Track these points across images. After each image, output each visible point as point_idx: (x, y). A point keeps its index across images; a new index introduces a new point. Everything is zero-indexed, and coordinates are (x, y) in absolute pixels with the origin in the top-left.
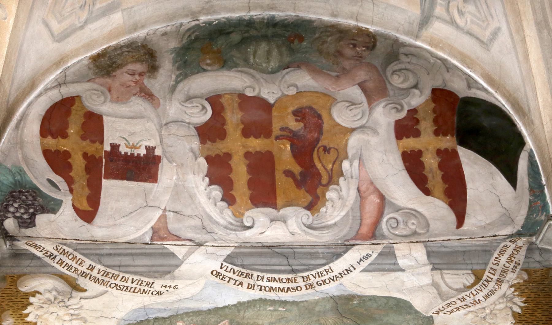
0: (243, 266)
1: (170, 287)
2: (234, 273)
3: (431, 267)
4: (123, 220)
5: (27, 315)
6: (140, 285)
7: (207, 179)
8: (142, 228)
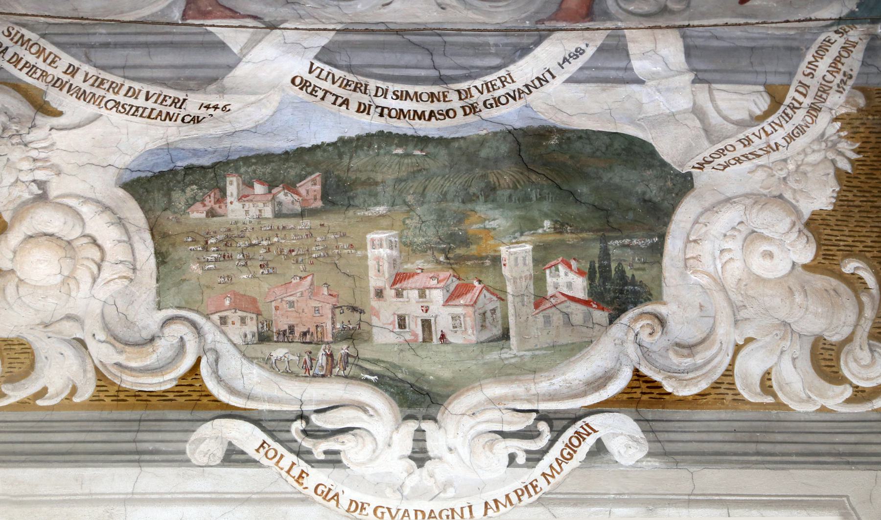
0: (350, 69)
2: (334, 83)
3: (690, 77)
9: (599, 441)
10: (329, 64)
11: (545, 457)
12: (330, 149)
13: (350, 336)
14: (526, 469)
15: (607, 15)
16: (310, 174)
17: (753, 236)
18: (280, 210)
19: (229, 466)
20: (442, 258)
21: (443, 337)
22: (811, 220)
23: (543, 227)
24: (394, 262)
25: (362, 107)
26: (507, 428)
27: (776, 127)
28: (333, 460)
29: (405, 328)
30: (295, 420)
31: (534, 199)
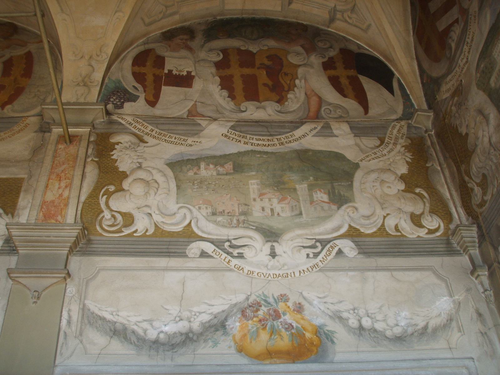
0: (241, 132)
1: (197, 142)
3: (353, 135)
5: (113, 155)
7: (220, 87)
9: (340, 249)
10: (234, 130)
11: (320, 255)
13: (244, 213)
14: (313, 259)
15: (324, 118)
16: (229, 162)
17: (383, 182)
19: (202, 258)
20: (276, 189)
21: (278, 214)
22: (401, 176)
23: (310, 179)
24: (259, 190)
25: (245, 143)
26: (305, 245)
28: (241, 256)
29: (264, 211)
30: (226, 242)
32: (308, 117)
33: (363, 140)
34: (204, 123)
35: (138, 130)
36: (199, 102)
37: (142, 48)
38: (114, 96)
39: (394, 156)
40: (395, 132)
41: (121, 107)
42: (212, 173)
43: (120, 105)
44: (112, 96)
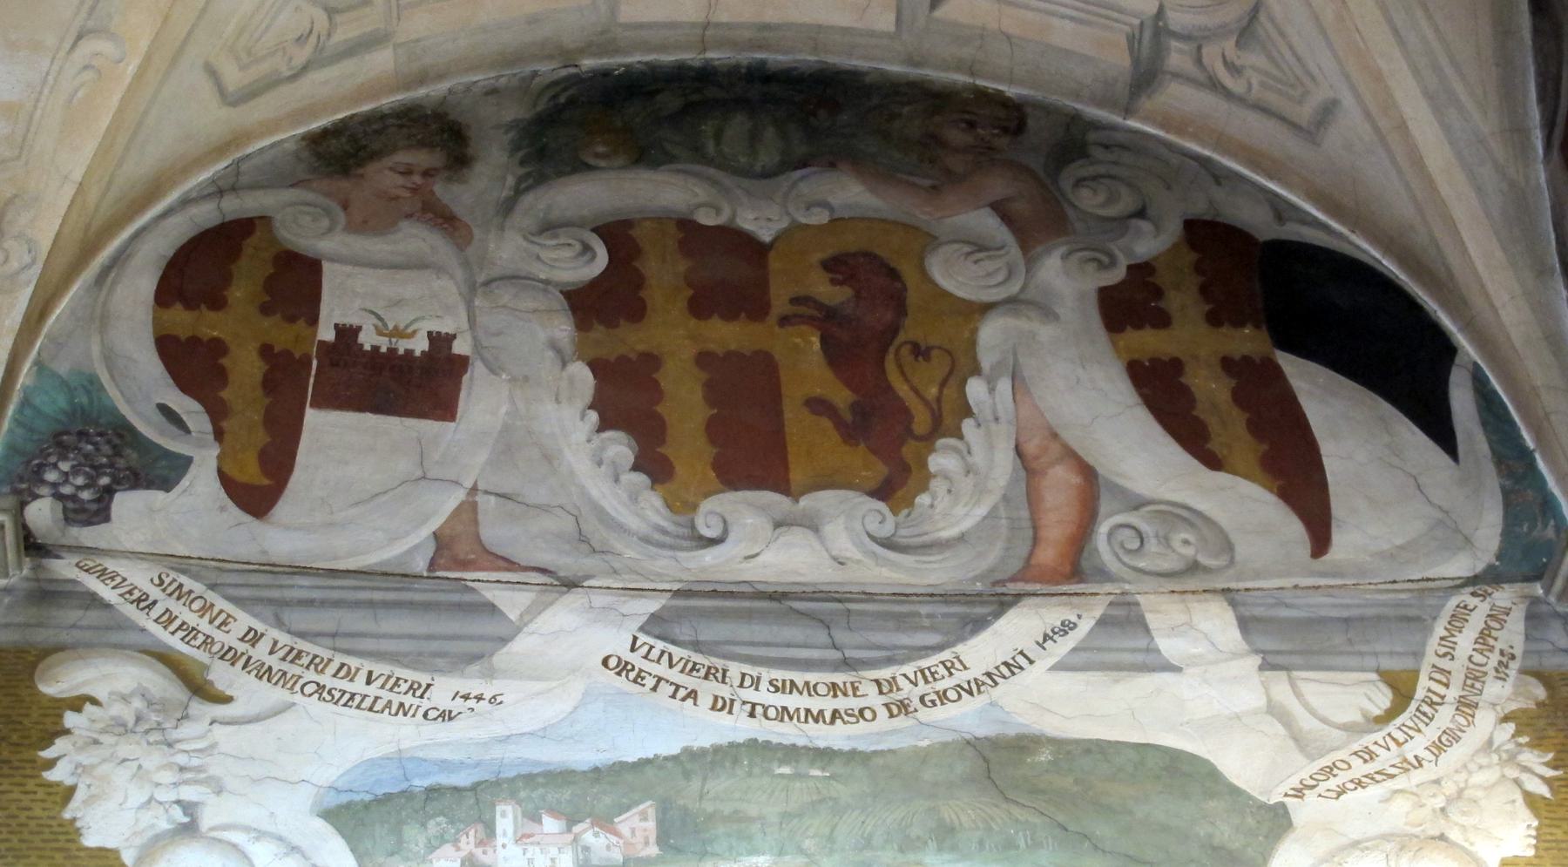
0: (696, 646)
1: (479, 698)
2: (671, 666)
3: (1257, 660)
4: (353, 511)
5: (51, 764)
6: (391, 690)
7: (593, 416)
8: (407, 534)
12: (670, 765)
15: (1104, 575)
16: (637, 803)
18: (587, 860)
27: (1411, 733)
31: (1022, 844)
32: (1028, 572)
33: (1305, 688)
34: (512, 602)
35: (181, 634)
36: (487, 492)
37: (206, 215)
38: (64, 458)
39: (1465, 766)
40: (1465, 642)
41: (99, 513)
42: (553, 860)
43: (94, 507)
44: (53, 459)
